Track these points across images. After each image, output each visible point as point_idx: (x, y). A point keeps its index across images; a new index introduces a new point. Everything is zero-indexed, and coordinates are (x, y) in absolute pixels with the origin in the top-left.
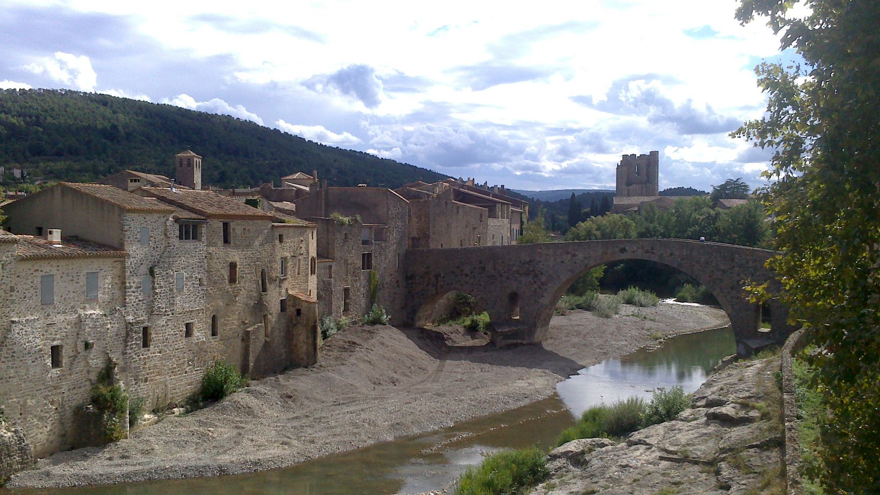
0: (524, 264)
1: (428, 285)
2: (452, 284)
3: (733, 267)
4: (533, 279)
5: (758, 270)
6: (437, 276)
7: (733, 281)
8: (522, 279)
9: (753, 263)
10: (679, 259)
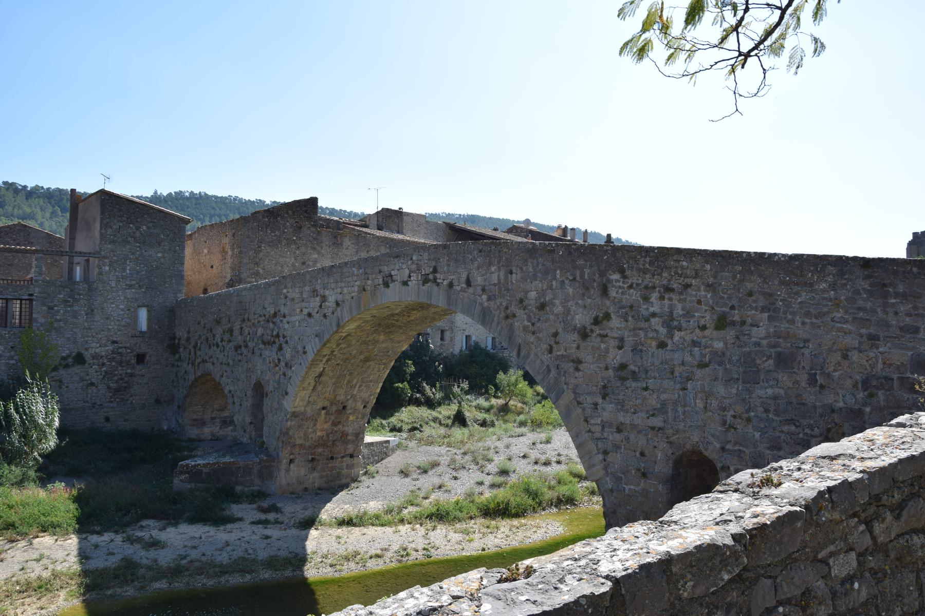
0: (268, 321)
1: (188, 364)
3: (607, 316)
4: (277, 354)
7: (607, 369)
9: (662, 298)
10: (484, 297)
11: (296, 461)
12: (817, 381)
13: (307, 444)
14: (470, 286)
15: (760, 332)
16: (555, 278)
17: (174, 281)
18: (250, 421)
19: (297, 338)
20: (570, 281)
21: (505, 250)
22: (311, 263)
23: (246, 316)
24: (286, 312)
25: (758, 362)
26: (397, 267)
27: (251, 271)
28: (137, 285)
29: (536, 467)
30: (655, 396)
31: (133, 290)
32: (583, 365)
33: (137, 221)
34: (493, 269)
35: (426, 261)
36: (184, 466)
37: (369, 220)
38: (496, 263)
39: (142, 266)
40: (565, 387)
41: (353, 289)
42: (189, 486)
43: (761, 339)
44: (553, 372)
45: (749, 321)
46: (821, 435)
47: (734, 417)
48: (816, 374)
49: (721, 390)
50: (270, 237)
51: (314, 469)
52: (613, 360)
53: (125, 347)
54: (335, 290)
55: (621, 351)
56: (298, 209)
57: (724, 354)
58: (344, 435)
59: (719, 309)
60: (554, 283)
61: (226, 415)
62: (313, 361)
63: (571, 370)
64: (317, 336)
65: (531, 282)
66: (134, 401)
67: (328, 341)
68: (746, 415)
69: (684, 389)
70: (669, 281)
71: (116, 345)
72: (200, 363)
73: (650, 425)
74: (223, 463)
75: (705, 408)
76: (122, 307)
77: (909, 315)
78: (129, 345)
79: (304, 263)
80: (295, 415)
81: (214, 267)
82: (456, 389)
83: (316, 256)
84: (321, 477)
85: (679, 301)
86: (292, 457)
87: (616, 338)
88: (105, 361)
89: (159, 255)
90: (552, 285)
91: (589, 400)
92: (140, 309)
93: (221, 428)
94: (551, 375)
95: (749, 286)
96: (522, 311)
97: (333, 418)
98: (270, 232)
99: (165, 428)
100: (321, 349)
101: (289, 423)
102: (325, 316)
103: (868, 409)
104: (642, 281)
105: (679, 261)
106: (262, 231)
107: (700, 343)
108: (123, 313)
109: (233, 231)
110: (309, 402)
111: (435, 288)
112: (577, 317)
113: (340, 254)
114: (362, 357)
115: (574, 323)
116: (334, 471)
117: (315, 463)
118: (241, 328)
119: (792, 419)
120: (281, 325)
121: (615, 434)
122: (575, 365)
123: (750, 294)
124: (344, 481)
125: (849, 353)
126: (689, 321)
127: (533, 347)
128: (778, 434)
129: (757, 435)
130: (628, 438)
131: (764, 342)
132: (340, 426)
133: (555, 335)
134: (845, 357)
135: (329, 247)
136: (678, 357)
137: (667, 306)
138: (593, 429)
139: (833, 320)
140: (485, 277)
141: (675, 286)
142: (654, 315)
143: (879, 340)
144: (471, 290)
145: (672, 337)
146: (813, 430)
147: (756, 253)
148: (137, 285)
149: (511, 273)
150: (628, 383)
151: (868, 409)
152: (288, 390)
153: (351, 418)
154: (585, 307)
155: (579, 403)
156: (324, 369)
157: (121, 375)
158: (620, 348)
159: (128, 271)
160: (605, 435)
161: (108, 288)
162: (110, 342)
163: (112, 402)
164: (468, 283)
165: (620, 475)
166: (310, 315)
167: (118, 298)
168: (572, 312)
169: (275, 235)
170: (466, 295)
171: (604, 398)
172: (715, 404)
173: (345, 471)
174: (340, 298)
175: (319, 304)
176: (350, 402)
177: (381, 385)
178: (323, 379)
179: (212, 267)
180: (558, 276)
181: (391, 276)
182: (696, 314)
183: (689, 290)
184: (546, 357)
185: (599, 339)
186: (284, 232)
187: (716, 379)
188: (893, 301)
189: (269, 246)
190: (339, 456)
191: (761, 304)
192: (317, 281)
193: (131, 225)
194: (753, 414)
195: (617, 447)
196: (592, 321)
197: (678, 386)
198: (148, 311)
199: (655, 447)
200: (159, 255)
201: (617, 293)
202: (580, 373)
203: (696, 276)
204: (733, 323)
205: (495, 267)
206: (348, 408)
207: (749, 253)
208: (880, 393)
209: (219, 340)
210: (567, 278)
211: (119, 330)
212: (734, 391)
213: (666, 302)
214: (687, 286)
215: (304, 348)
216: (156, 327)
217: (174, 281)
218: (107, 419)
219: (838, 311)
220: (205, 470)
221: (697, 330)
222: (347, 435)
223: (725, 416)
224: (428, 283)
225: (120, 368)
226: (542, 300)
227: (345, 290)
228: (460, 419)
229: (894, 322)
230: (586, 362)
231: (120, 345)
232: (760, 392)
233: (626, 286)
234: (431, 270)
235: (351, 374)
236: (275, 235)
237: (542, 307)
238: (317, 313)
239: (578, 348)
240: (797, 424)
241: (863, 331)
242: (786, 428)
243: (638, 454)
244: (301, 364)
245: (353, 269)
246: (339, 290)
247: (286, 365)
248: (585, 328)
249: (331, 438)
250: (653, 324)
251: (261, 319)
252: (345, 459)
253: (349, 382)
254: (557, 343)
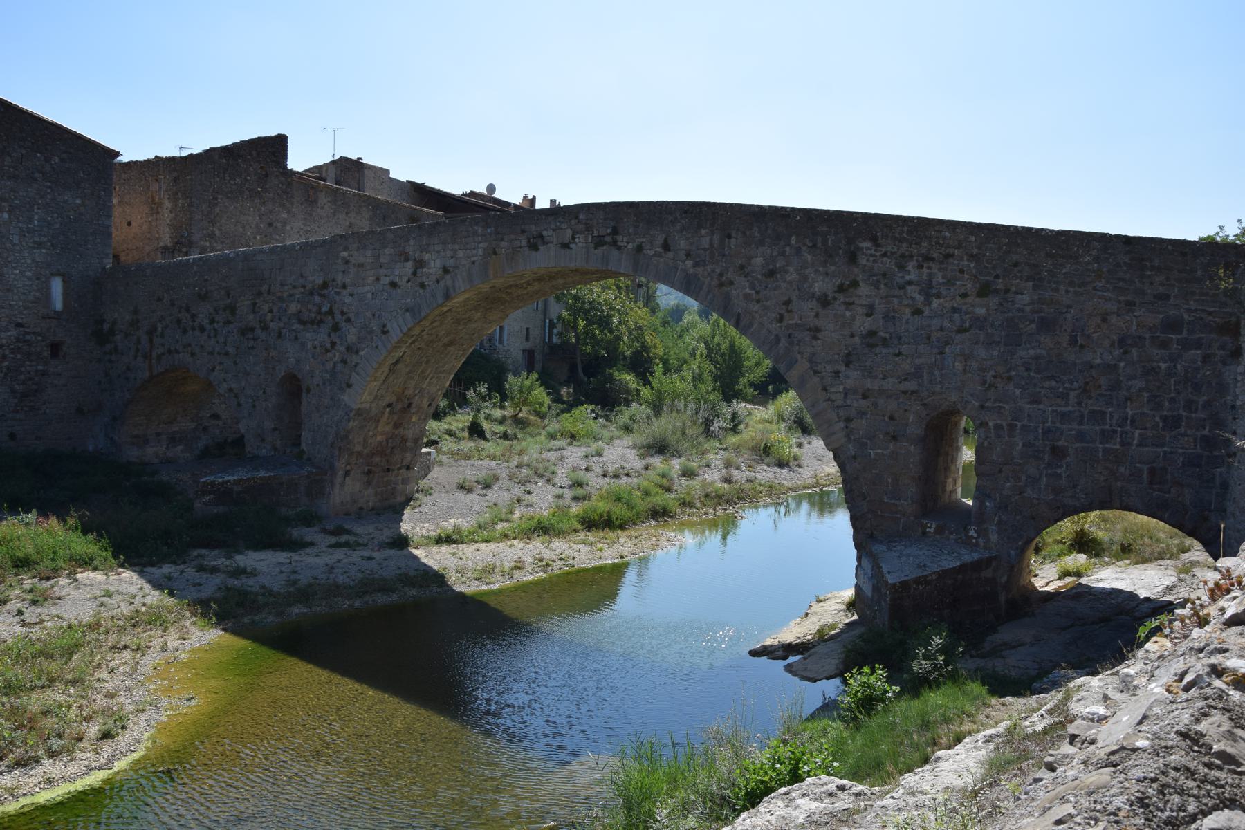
0: (311, 294)
1: (136, 357)
2: (178, 352)
3: (855, 284)
4: (329, 335)
5: (938, 296)
6: (151, 332)
7: (852, 336)
8: (308, 335)
9: (920, 267)
10: (689, 263)
11: (352, 473)
12: (1077, 341)
13: (365, 451)
14: (669, 250)
15: (1026, 299)
16: (789, 244)
17: (98, 240)
18: (273, 426)
19: (368, 314)
20: (809, 247)
21: (721, 212)
22: (279, 225)
23: (265, 287)
24: (347, 281)
25: (1021, 326)
26: (553, 226)
27: (205, 232)
28: (49, 244)
29: (607, 480)
30: (909, 361)
31: (44, 251)
32: (823, 333)
33: (46, 149)
34: (703, 232)
35: (601, 221)
36: (208, 484)
37: (327, 171)
38: (708, 225)
39: (55, 215)
40: (799, 357)
41: (475, 252)
42: (215, 511)
43: (1024, 305)
44: (783, 342)
45: (1013, 289)
46: (1080, 387)
47: (994, 377)
48: (1077, 335)
49: (982, 353)
50: (228, 185)
51: (369, 483)
52: (860, 328)
53: (34, 333)
54: (443, 254)
55: (869, 319)
56: (264, 149)
57: (985, 319)
58: (404, 440)
59: (982, 278)
60: (788, 249)
61: (174, 429)
62: (399, 342)
63: (807, 339)
64: (407, 310)
65: (757, 248)
66: (48, 411)
67: (425, 318)
68: (1007, 375)
69: (941, 353)
70: (929, 250)
71: (21, 329)
72: (163, 354)
73: (902, 389)
74: (261, 478)
75: (964, 370)
76: (28, 274)
77: (1162, 284)
78: (39, 329)
80: (359, 413)
81: (133, 224)
82: (470, 394)
84: (376, 494)
85: (940, 269)
86: (348, 467)
87: (865, 306)
88: (7, 352)
89: (78, 201)
90: (785, 251)
91: (828, 367)
92: (53, 278)
93: (167, 448)
94: (781, 345)
95: (1015, 257)
96: (743, 279)
97: (396, 417)
98: (228, 178)
99: (91, 448)
100: (414, 327)
101: (351, 423)
102: (422, 285)
103: (1122, 364)
104: (898, 249)
105: (941, 232)
106: (218, 177)
107: (961, 309)
108: (30, 283)
109: (175, 174)
110: (376, 396)
111: (615, 252)
112: (816, 284)
113: (314, 214)
114: (446, 340)
115: (812, 290)
116: (389, 487)
117: (371, 476)
118: (254, 304)
119: (1053, 376)
120: (337, 298)
121: (861, 401)
122: (812, 333)
123: (1016, 264)
124: (400, 499)
125: (1108, 317)
126: (950, 289)
127: (757, 316)
128: (1038, 390)
129: (1018, 392)
130: (876, 404)
131: (1028, 309)
132: (401, 430)
133: (788, 303)
134: (1104, 320)
135: (302, 204)
136: (936, 323)
137: (925, 274)
138: (833, 397)
139: (1094, 288)
140: (692, 241)
141: (935, 255)
142: (910, 283)
143: (1135, 305)
144: (670, 255)
145: (930, 304)
146: (1072, 384)
147: (1023, 228)
148: (49, 244)
149: (729, 237)
150: (877, 350)
151: (1122, 364)
152: (352, 381)
153: (414, 419)
154: (827, 274)
155: (816, 372)
156: (405, 353)
157: (29, 373)
158: (869, 315)
159: (36, 222)
160: (849, 402)
161: (8, 245)
162: (13, 325)
163: (17, 412)
164: (666, 247)
165: (865, 441)
166: (393, 285)
167: (23, 261)
168: (810, 280)
169: (235, 184)
170: (662, 260)
171: (847, 365)
172: (974, 365)
173: (400, 487)
174: (450, 263)
175: (411, 270)
176: (417, 398)
177: (452, 376)
178: (399, 366)
179: (129, 224)
180: (793, 242)
181: (541, 237)
182: (958, 283)
183: (951, 260)
184: (775, 327)
185: (843, 307)
186: (246, 179)
187: (977, 343)
188: (1149, 273)
189: (228, 198)
190: (396, 467)
191: (1026, 274)
192: (408, 241)
193: (38, 155)
194: (1014, 373)
195: (862, 414)
196: (836, 289)
197: (936, 351)
198: (64, 281)
199: (906, 410)
200: (78, 201)
201: (868, 260)
202: (819, 341)
203: (959, 246)
204: (997, 291)
205: (707, 230)
206: (414, 405)
207: (1016, 228)
208: (1134, 350)
209: (206, 321)
210: (804, 245)
211: (26, 308)
212: (995, 353)
213: (925, 270)
214: (948, 256)
215: (384, 326)
216: (76, 305)
217: (98, 240)
218: (12, 436)
219: (1100, 281)
220: (236, 489)
221: (958, 298)
222: (406, 441)
223: (986, 376)
224: (603, 245)
225: (27, 363)
226: (771, 267)
227: (461, 254)
228: (476, 431)
229: (1149, 291)
230: (826, 330)
231: (27, 330)
232: (1023, 353)
233: (878, 254)
234: (609, 231)
235: (428, 362)
236: (235, 184)
237: (771, 274)
238: (408, 282)
239: (817, 316)
240: (1058, 380)
241: (1122, 298)
242: (1047, 384)
243: (887, 419)
244: (377, 347)
245: (476, 228)
246: (449, 253)
247: (349, 349)
248: (826, 296)
249: (390, 445)
250: (909, 291)
251: (295, 291)
252: (401, 471)
253: (423, 372)
254: (789, 311)
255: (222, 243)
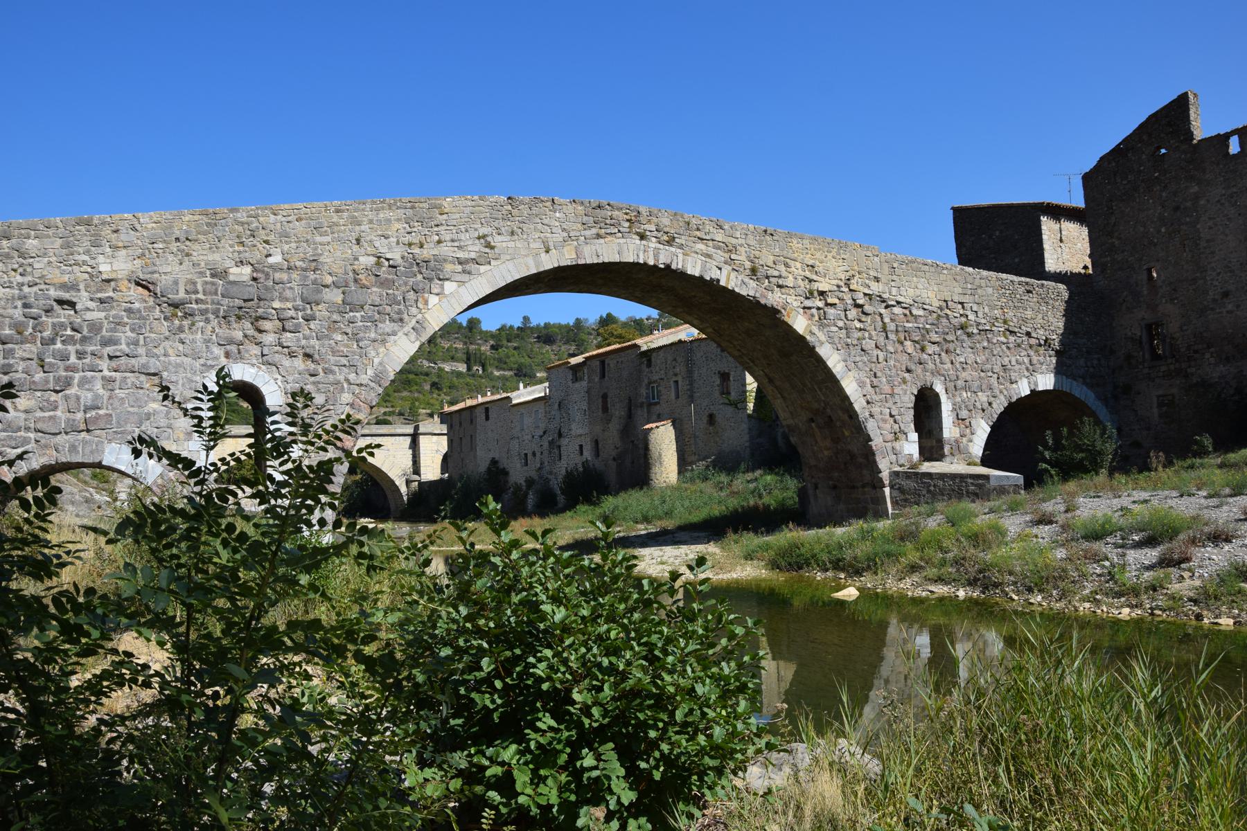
22: (1189, 204)
58: (853, 456)
79: (1177, 208)
83: (1196, 189)
89: (1017, 260)
110: (791, 413)
153: (847, 433)
200: (1017, 260)
252: (866, 489)
255: (1123, 252)
